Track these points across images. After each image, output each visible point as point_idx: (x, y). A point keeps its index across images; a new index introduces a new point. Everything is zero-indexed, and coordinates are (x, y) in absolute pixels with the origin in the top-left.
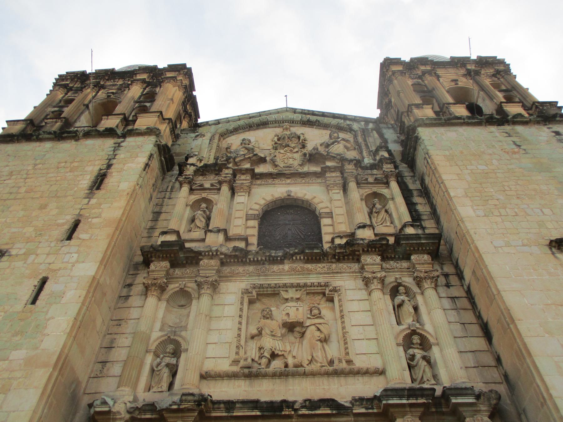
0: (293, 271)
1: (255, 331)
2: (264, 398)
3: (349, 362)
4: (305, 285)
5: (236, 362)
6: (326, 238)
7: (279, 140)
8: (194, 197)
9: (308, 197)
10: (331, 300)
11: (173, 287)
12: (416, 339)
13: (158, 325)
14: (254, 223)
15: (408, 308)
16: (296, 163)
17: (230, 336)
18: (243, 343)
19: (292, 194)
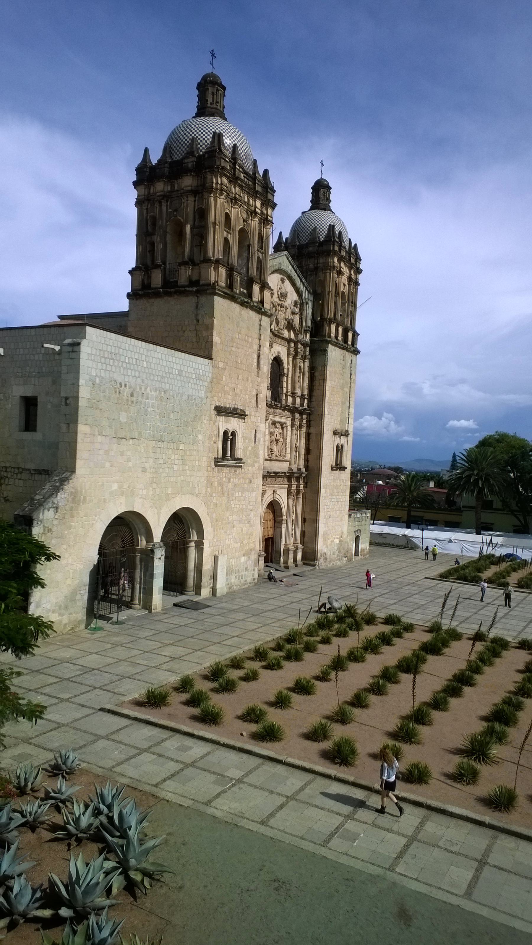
2: (277, 470)
6: (285, 391)
9: (283, 358)
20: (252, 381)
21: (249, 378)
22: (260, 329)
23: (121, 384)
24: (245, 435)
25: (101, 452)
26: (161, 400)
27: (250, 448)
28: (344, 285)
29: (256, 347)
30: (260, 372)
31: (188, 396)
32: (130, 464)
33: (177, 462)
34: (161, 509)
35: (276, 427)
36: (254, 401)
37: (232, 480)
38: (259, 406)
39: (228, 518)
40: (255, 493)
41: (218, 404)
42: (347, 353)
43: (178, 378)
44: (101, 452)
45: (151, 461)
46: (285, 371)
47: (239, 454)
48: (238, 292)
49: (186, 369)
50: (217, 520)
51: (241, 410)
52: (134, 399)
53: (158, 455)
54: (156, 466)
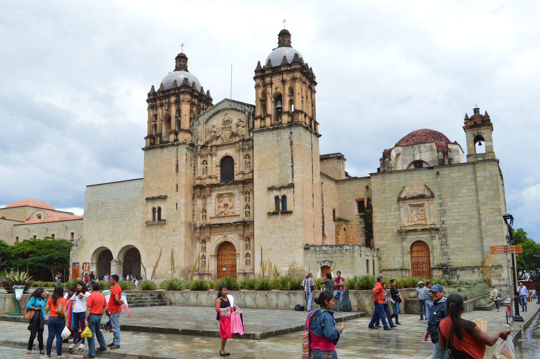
0: (226, 188)
1: (219, 206)
3: (235, 213)
4: (228, 193)
5: (215, 214)
6: (235, 173)
7: (223, 122)
8: (203, 160)
10: (234, 196)
11: (202, 194)
12: (248, 206)
13: (201, 206)
14: (219, 168)
15: (248, 198)
16: (228, 136)
17: (214, 208)
18: (217, 209)
19: (227, 154)
20: (172, 180)
21: (170, 179)
22: (177, 153)
23: (98, 201)
24: (167, 207)
25: (91, 226)
26: (116, 203)
27: (172, 213)
28: (276, 88)
29: (174, 163)
30: (179, 173)
31: (130, 198)
32: (102, 229)
33: (124, 226)
34: (116, 246)
35: (225, 197)
36: (175, 189)
37: (159, 231)
38: (180, 190)
39: (157, 250)
40: (178, 237)
41: (148, 197)
42: (282, 131)
43: (124, 192)
44: (91, 226)
45: (111, 227)
46: (235, 162)
47: (163, 217)
48: (158, 143)
49: (128, 187)
50: (149, 251)
51: (164, 196)
52: (104, 205)
53: (114, 225)
54: (113, 229)
